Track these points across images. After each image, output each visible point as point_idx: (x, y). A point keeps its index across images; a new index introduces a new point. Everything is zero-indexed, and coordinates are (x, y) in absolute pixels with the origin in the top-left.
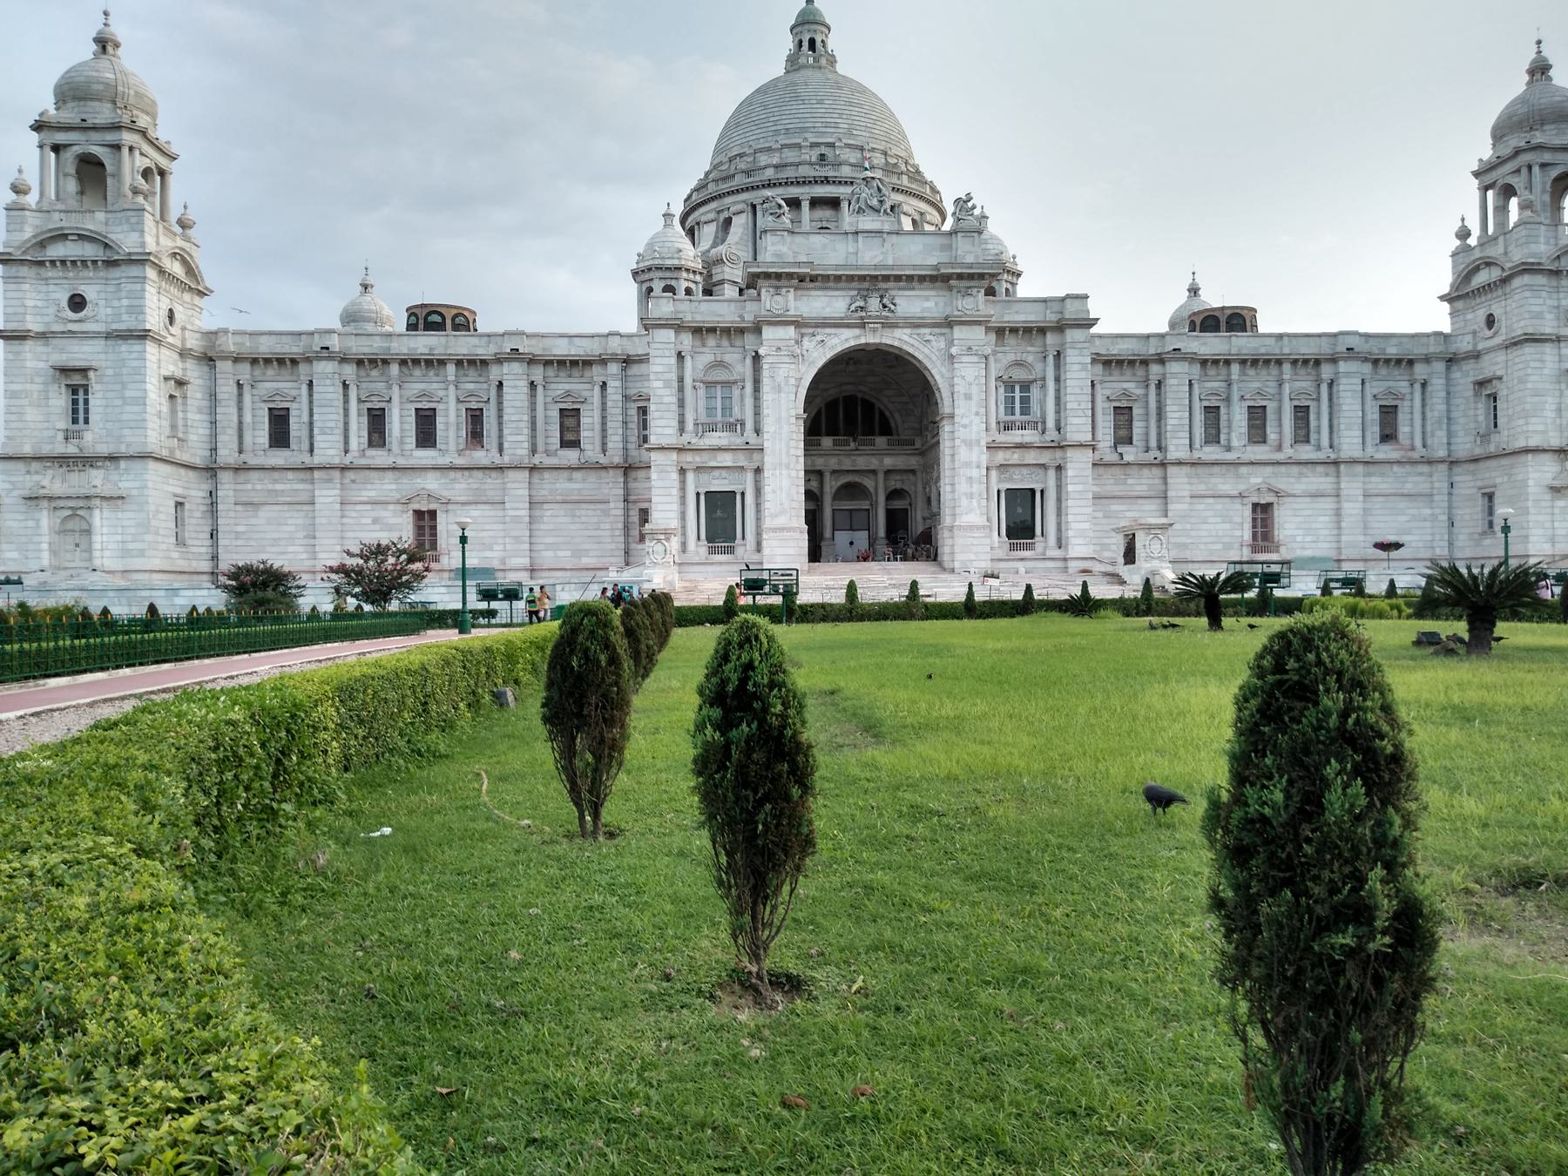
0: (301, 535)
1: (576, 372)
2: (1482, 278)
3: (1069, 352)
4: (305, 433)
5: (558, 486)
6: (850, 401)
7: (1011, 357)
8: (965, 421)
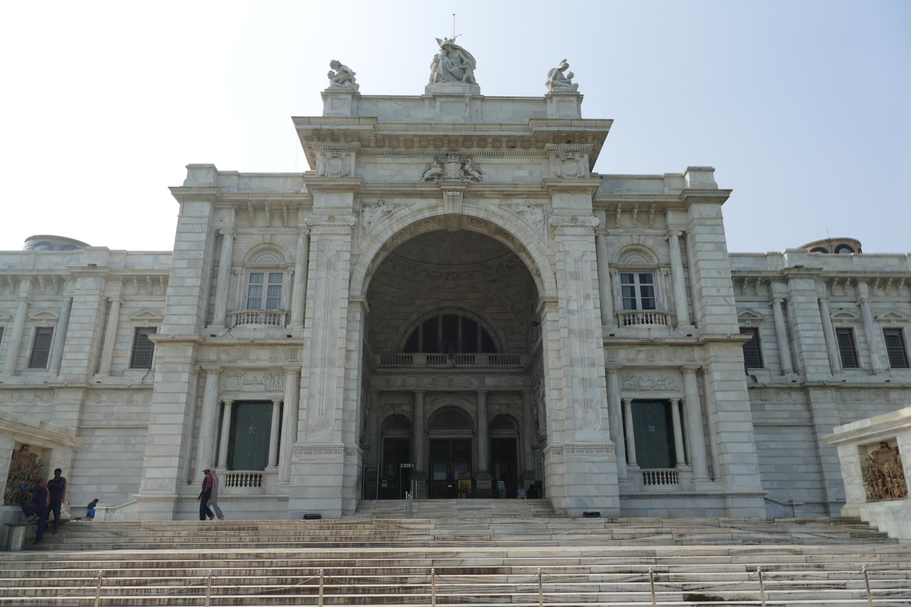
3: (698, 229)
5: (115, 409)
6: (450, 320)
7: (626, 240)
8: (573, 306)
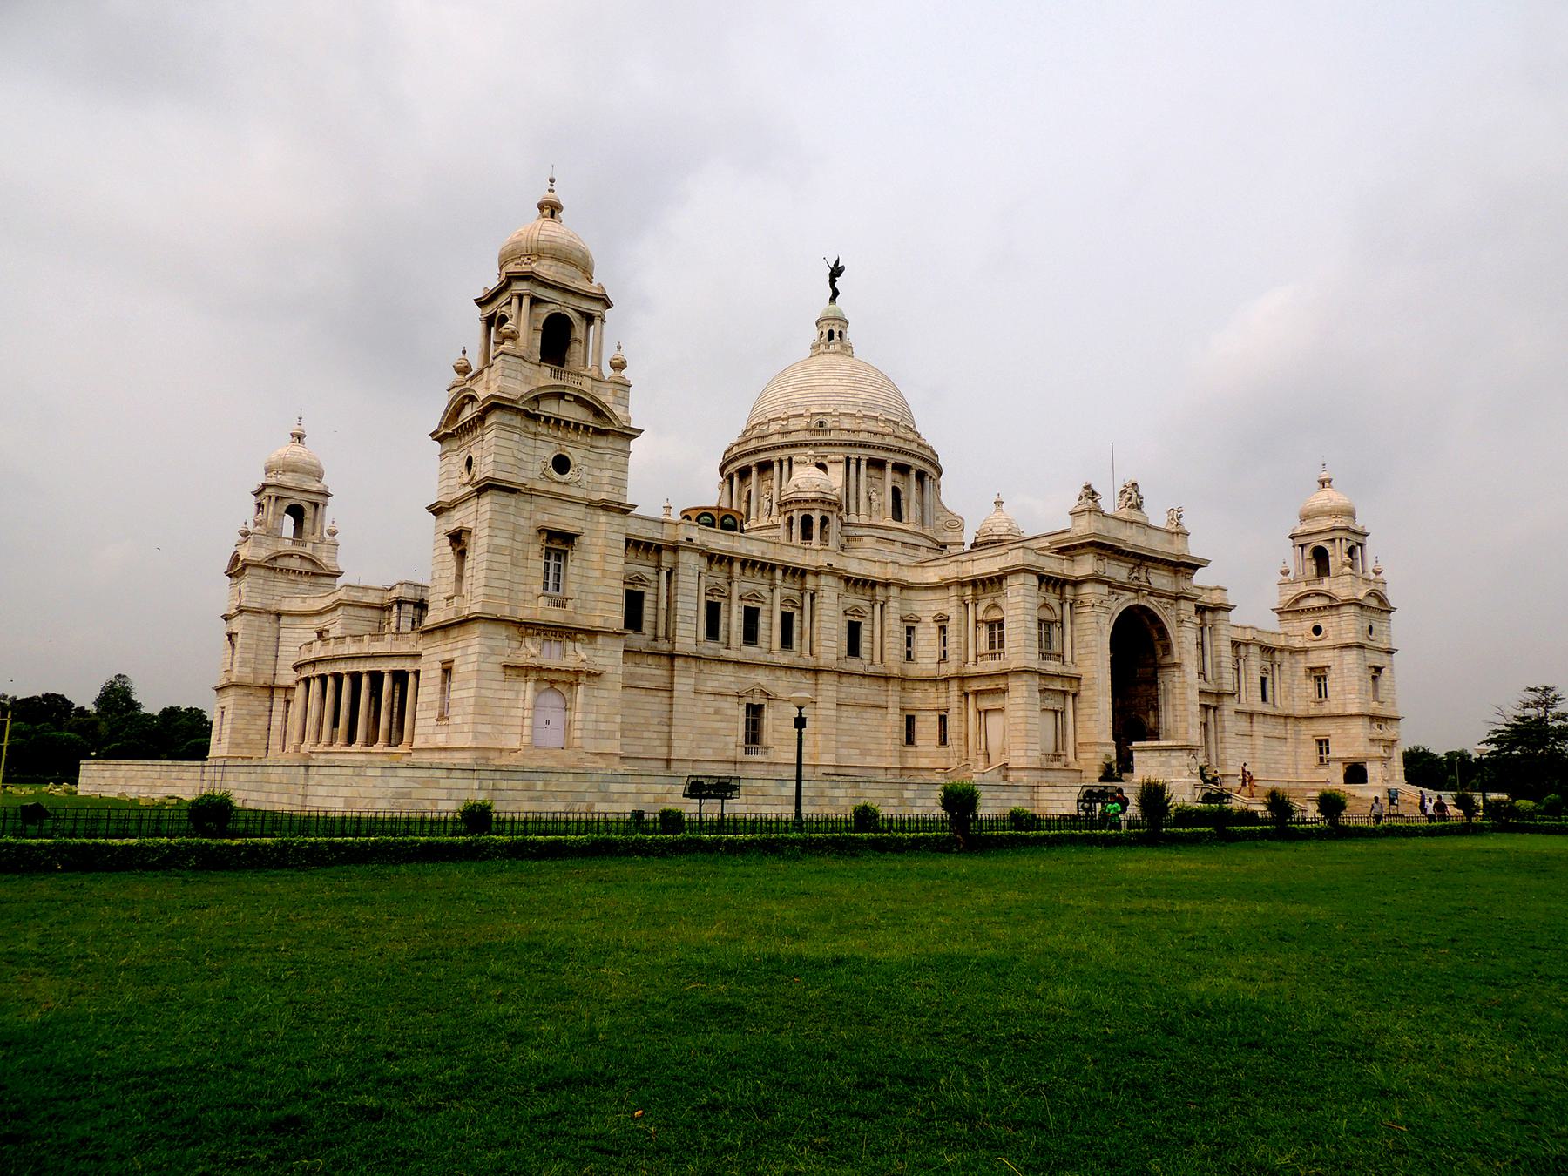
0: (656, 720)
1: (859, 589)
2: (1313, 602)
4: (662, 619)
